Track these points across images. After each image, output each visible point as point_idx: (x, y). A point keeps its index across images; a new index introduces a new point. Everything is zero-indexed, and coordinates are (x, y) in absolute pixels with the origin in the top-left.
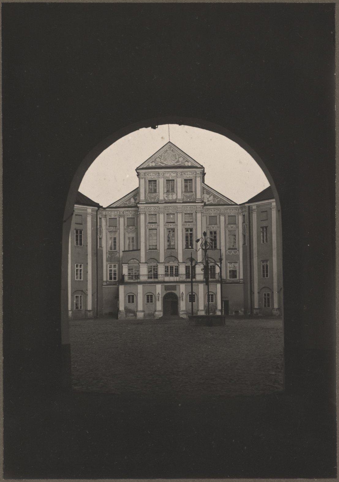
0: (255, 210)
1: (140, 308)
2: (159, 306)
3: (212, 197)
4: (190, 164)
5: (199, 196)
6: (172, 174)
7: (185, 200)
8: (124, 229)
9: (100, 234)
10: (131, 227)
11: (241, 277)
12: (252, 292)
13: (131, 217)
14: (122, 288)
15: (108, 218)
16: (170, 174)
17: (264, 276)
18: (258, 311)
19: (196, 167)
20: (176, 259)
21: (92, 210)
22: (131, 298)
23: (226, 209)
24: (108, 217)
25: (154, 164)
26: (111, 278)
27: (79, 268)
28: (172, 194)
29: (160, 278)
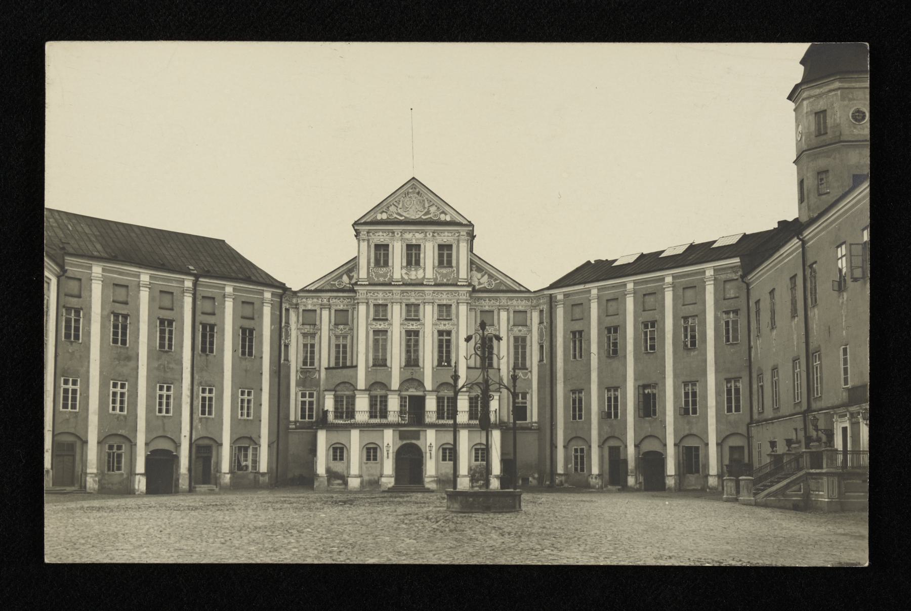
0: (560, 301)
1: (354, 469)
2: (389, 467)
3: (486, 276)
4: (448, 219)
5: (463, 274)
6: (417, 235)
7: (438, 281)
8: (330, 330)
9: (286, 338)
10: (342, 327)
11: (535, 419)
12: (553, 446)
13: (341, 307)
14: (322, 437)
15: (301, 311)
16: (414, 237)
17: (574, 418)
18: (563, 478)
19: (460, 224)
20: (421, 384)
21: (273, 294)
22: (339, 452)
23: (511, 299)
24: (301, 308)
25: (385, 216)
26: (303, 417)
27: (164, 392)
28: (416, 270)
29: (393, 418)
